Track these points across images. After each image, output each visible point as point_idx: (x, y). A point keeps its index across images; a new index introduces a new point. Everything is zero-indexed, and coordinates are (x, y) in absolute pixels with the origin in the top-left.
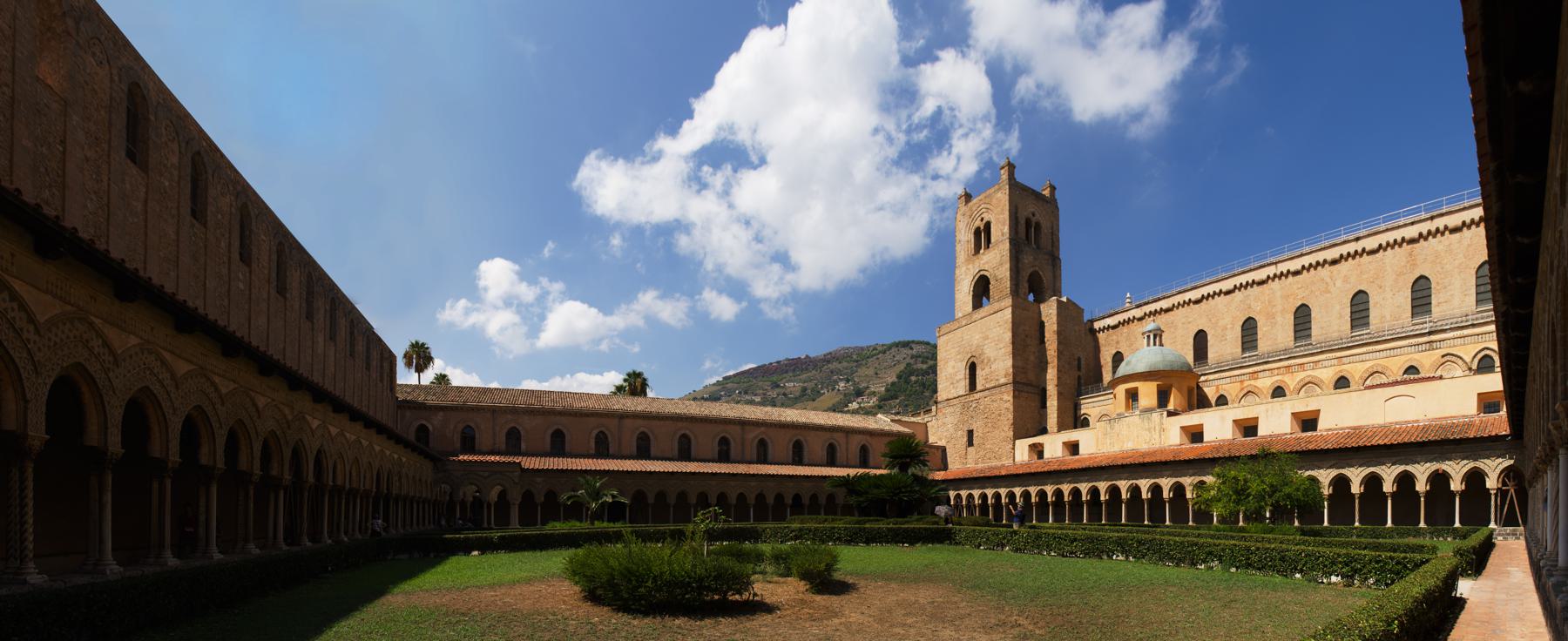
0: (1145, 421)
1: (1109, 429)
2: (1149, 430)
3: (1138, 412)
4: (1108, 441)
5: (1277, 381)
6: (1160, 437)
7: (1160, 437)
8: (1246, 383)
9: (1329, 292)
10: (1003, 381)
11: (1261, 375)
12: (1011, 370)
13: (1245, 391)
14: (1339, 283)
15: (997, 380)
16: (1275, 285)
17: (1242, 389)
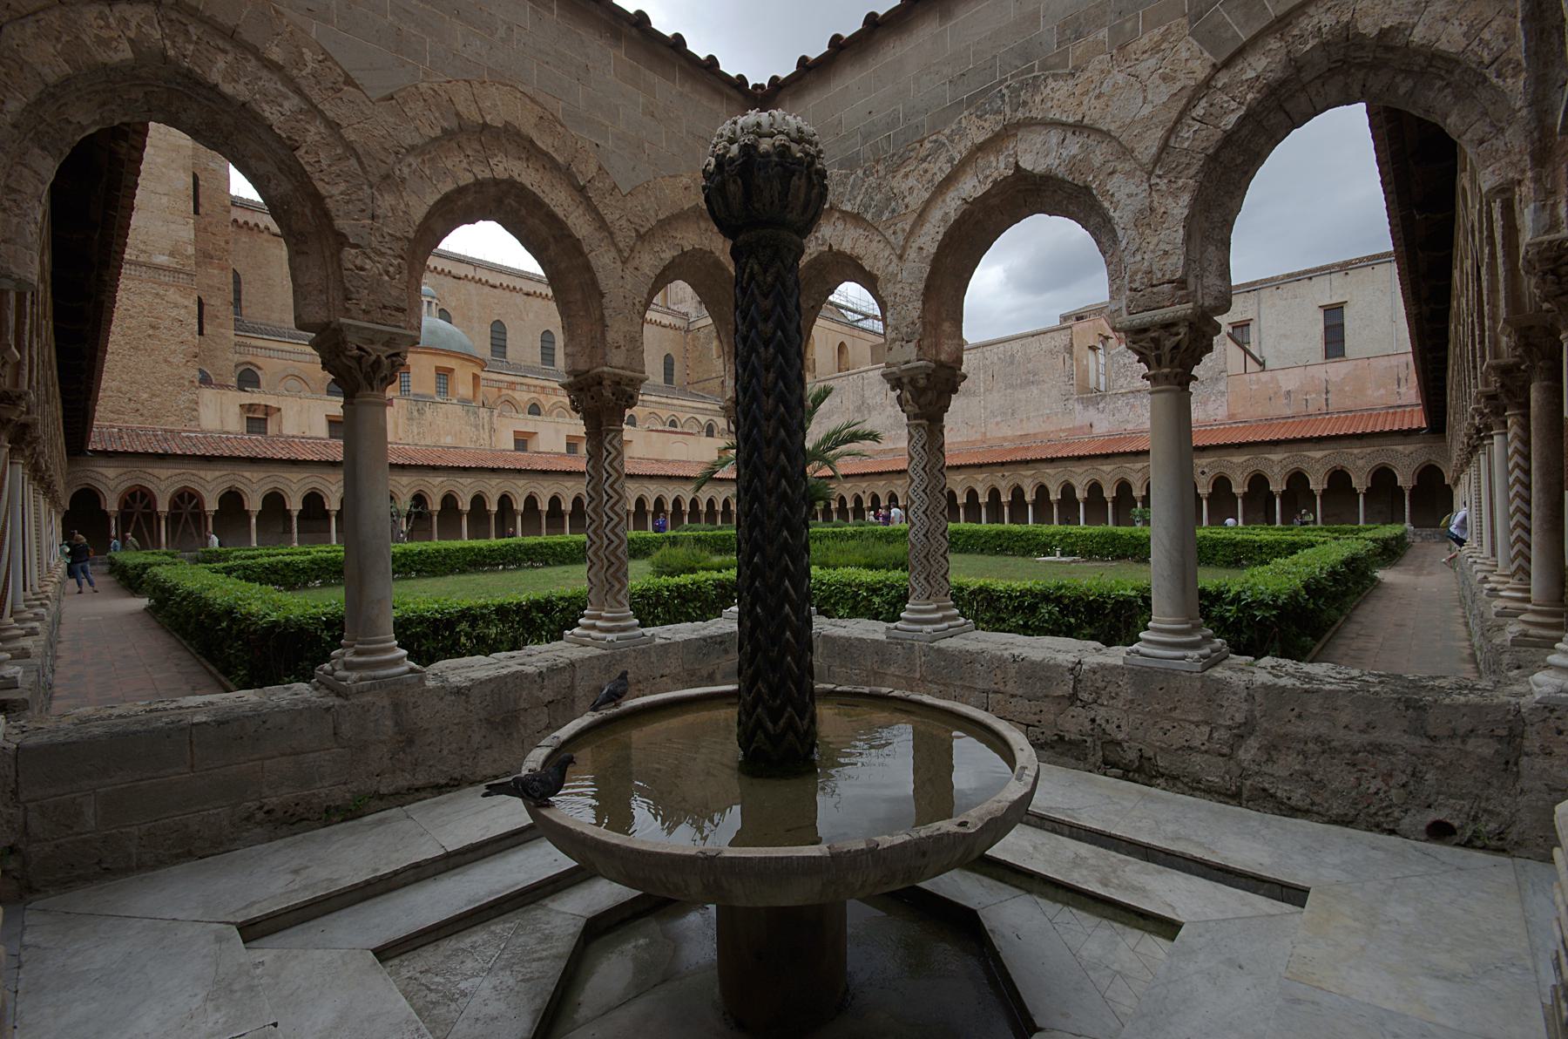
0: (470, 414)
1: (416, 413)
2: (476, 426)
3: (455, 401)
4: (416, 431)
5: (533, 398)
6: (491, 438)
7: (491, 438)
8: (504, 391)
9: (523, 320)
10: (162, 259)
11: (518, 387)
12: (191, 250)
13: (503, 399)
14: (531, 316)
15: (144, 252)
16: (471, 286)
17: (500, 397)
